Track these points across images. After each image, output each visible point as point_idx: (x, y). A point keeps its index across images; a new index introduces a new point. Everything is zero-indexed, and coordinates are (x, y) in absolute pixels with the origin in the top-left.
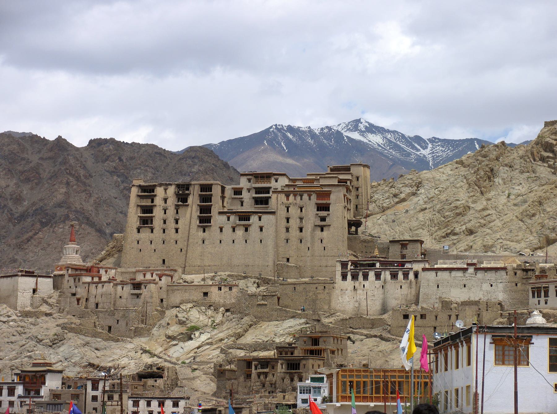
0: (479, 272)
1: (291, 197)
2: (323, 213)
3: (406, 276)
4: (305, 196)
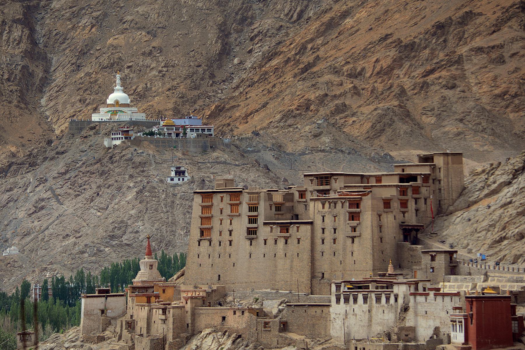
0: (438, 297)
1: (327, 205)
2: (354, 223)
3: (388, 299)
4: (339, 205)
